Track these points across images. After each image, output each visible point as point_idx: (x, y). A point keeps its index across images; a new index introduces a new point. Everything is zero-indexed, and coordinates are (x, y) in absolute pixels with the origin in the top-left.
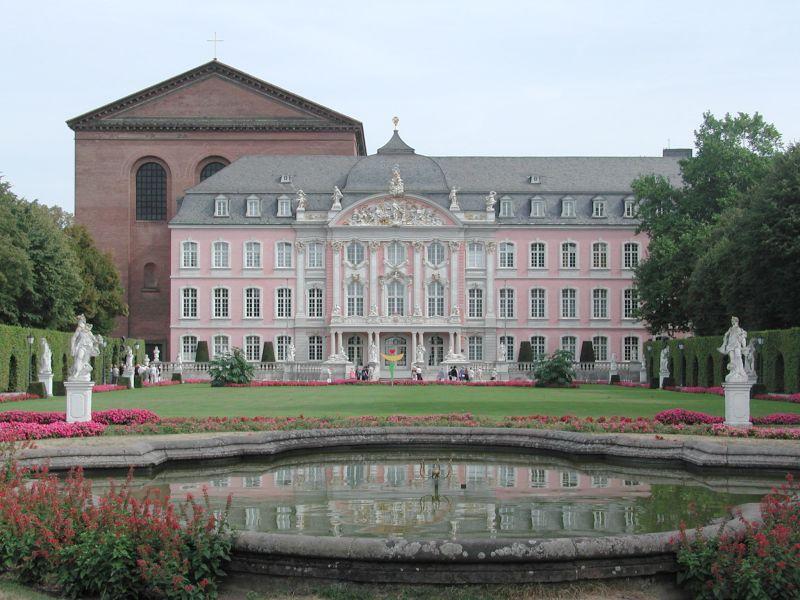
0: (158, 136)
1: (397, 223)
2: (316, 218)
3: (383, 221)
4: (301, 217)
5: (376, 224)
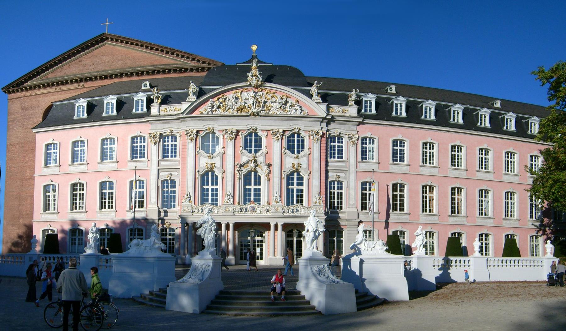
3: (241, 109)
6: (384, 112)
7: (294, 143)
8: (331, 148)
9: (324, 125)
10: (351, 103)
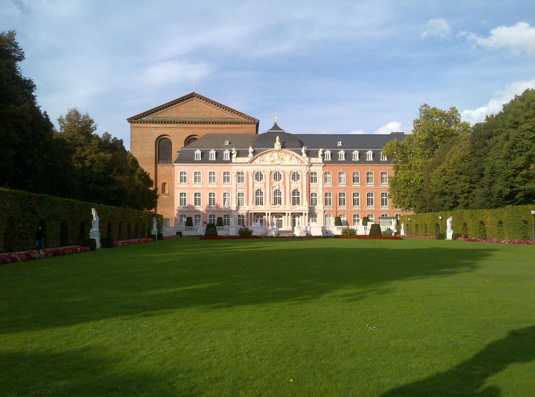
0: (168, 125)
1: (277, 162)
2: (241, 160)
4: (234, 160)
5: (268, 163)
8: (311, 178)
9: (308, 168)
10: (320, 156)
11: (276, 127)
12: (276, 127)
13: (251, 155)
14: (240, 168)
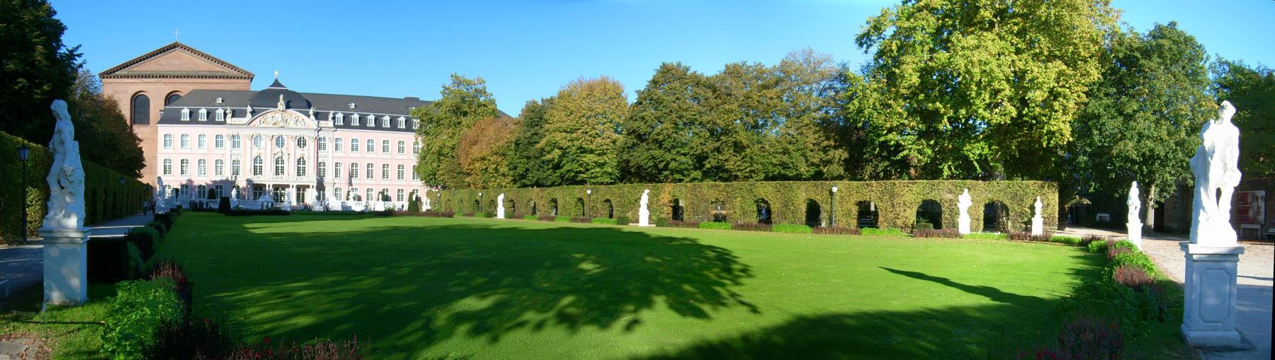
2: (237, 120)
4: (229, 120)
6: (347, 124)
7: (301, 142)
8: (320, 145)
11: (276, 83)
12: (276, 83)
13: (249, 115)
14: (234, 131)
